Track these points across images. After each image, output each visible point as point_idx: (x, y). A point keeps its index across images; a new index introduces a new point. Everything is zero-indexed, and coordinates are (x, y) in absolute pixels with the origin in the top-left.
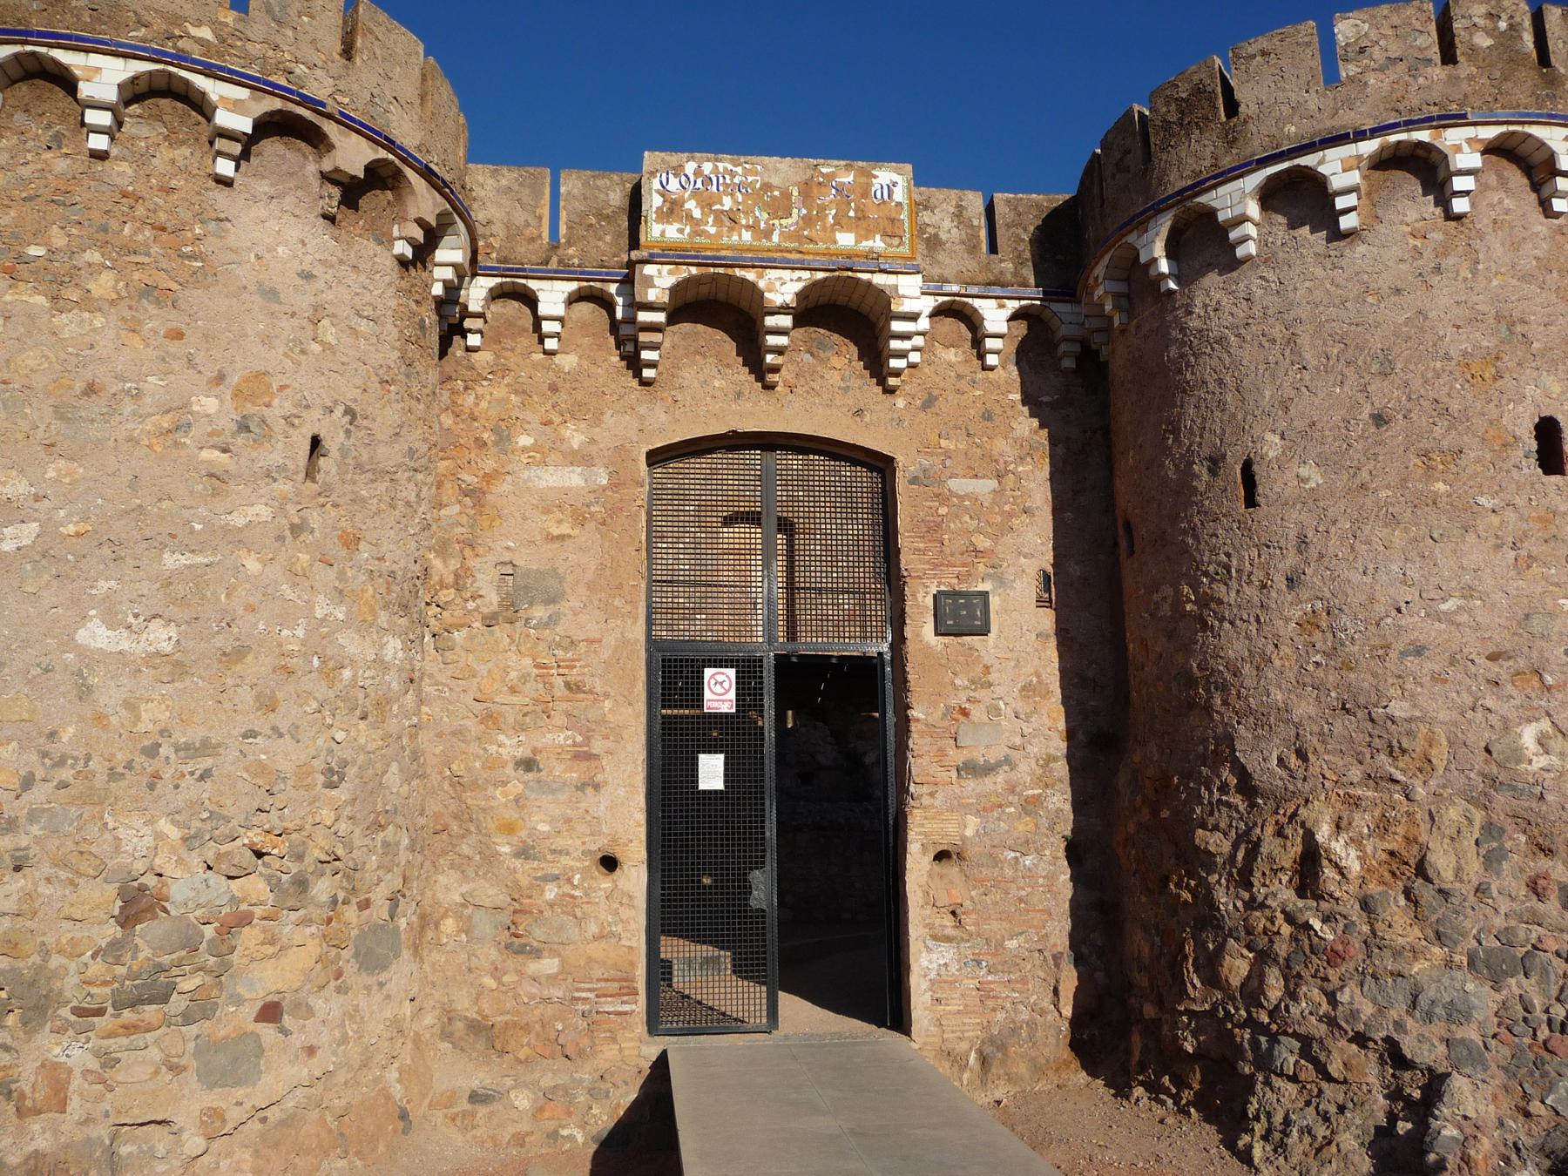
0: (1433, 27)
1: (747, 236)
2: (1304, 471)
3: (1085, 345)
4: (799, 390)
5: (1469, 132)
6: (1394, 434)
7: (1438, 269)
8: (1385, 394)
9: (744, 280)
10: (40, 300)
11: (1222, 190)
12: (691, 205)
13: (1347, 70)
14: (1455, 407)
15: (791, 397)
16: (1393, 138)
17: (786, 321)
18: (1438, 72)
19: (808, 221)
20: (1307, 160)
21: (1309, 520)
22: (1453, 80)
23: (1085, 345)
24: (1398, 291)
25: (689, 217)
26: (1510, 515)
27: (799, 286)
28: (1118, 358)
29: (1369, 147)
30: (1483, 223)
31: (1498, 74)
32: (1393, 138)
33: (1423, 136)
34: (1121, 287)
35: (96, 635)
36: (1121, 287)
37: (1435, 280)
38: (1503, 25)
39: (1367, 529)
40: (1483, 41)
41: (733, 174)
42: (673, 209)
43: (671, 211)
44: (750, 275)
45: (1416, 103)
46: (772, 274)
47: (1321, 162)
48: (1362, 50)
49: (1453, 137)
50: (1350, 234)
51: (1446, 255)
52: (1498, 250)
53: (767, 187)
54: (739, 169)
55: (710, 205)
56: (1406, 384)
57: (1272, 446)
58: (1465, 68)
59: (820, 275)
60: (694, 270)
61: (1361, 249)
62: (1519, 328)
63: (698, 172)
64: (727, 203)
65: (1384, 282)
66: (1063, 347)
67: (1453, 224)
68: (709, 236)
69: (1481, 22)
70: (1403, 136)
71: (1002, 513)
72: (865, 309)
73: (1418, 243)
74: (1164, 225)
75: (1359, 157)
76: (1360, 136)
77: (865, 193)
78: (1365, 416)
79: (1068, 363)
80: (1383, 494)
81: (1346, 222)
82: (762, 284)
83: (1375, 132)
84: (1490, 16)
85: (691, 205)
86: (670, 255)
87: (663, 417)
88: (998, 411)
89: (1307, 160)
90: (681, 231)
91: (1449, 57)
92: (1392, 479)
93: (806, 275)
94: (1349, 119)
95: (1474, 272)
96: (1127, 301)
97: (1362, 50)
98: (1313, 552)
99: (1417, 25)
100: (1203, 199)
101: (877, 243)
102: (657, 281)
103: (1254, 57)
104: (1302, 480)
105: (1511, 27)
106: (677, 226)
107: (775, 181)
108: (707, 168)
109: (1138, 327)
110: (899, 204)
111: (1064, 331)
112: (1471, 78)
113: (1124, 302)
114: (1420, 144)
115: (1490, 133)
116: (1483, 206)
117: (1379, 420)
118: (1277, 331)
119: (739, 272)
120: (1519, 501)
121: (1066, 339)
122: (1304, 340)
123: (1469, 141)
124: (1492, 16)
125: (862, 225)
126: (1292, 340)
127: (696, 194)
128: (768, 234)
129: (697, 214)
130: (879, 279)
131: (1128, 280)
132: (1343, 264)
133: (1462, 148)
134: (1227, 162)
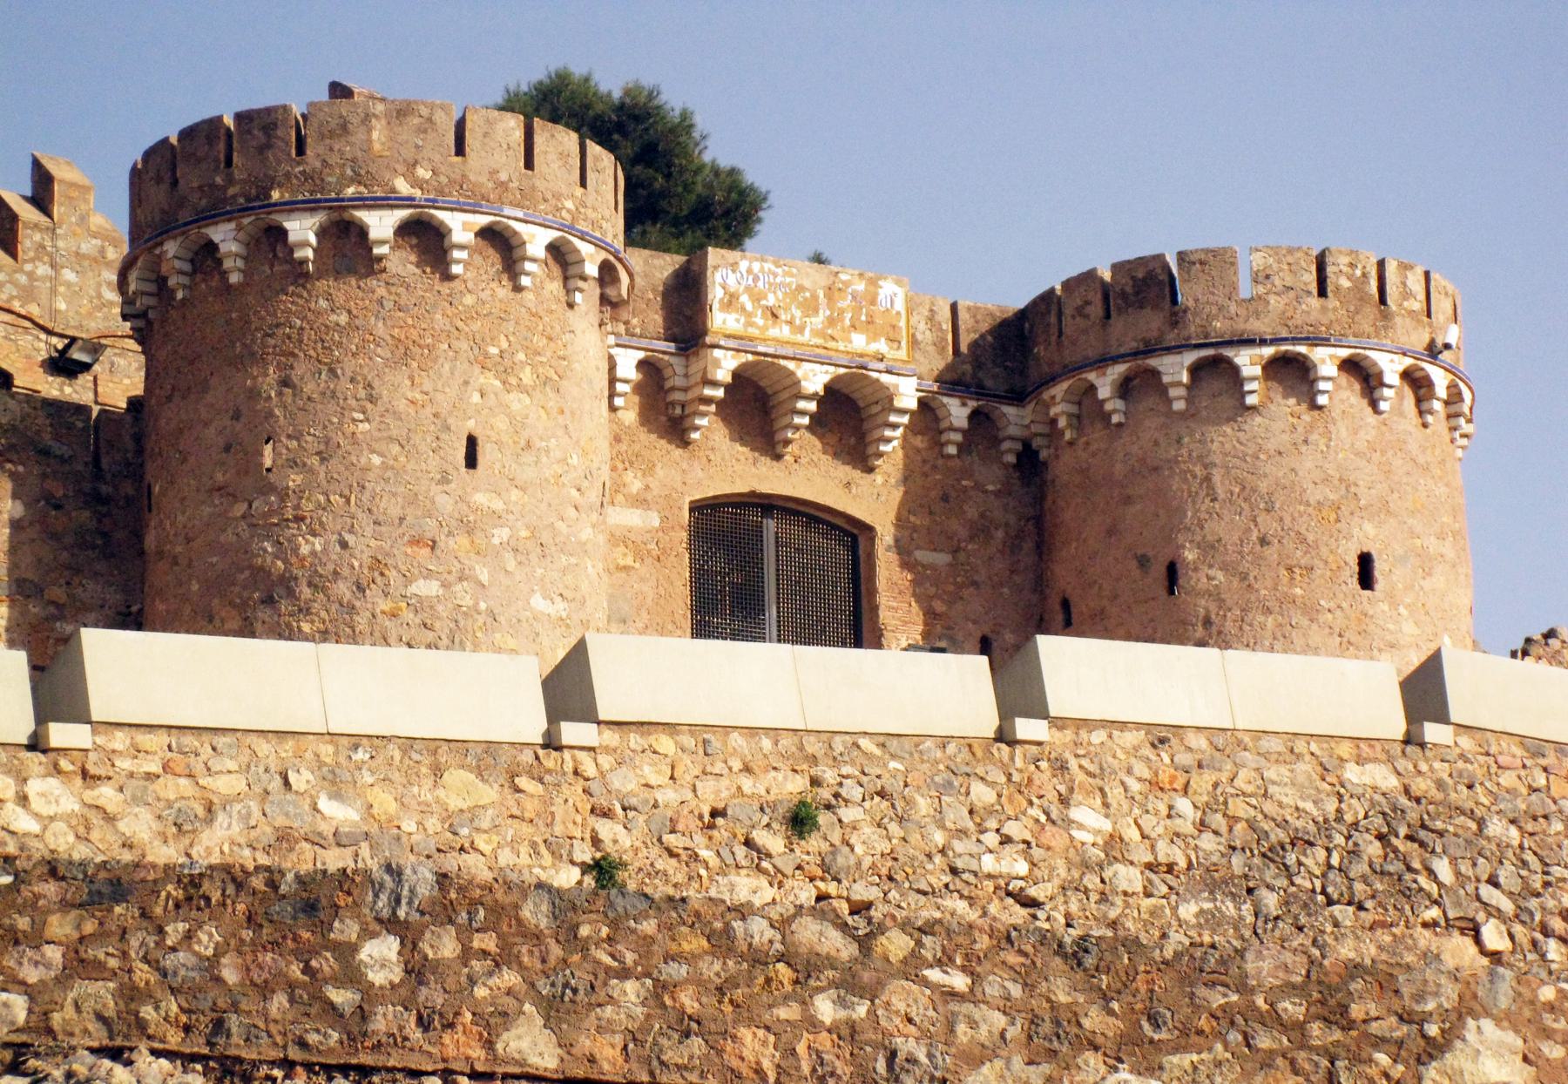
0: (1314, 268)
1: (786, 329)
2: (1212, 572)
3: (1027, 444)
4: (803, 461)
5: (1332, 350)
6: (1271, 553)
7: (1306, 441)
8: (1268, 524)
9: (785, 368)
10: (497, 383)
12: (744, 299)
14: (1311, 538)
15: (796, 466)
16: (1284, 348)
18: (1314, 302)
19: (831, 321)
20: (1228, 352)
21: (1213, 607)
22: (1324, 309)
23: (1027, 444)
25: (743, 309)
26: (1338, 613)
27: (826, 378)
28: (1063, 468)
29: (1268, 351)
30: (1336, 413)
31: (1352, 308)
33: (1302, 349)
34: (1074, 409)
35: (539, 603)
36: (1074, 409)
37: (1304, 448)
38: (1358, 273)
39: (1250, 616)
40: (1345, 283)
41: (776, 275)
42: (731, 302)
43: (730, 302)
44: (791, 365)
45: (1299, 322)
46: (806, 365)
48: (1267, 277)
50: (1253, 408)
52: (1344, 433)
53: (800, 288)
54: (779, 271)
55: (759, 300)
56: (1281, 519)
57: (1190, 555)
58: (1332, 302)
59: (842, 371)
60: (750, 357)
61: (1258, 419)
62: (1353, 489)
63: (749, 271)
64: (771, 300)
65: (1271, 446)
66: (1006, 445)
67: (1316, 413)
68: (758, 327)
69: (1345, 269)
70: (1290, 348)
71: (955, 583)
72: (855, 396)
73: (1295, 421)
75: (1261, 357)
76: (1263, 342)
77: (873, 302)
78: (1254, 538)
79: (1011, 459)
80: (1263, 592)
81: (1251, 400)
82: (799, 374)
83: (1275, 341)
84: (1351, 265)
85: (744, 299)
87: (701, 474)
88: (954, 494)
90: (738, 321)
91: (1322, 293)
92: (1269, 583)
93: (832, 369)
94: (1258, 326)
95: (1328, 447)
96: (1077, 420)
97: (1267, 277)
98: (1214, 629)
99: (1304, 264)
100: (1153, 362)
101: (882, 346)
102: (724, 363)
104: (1209, 578)
105: (1364, 275)
106: (734, 316)
107: (807, 283)
108: (756, 266)
109: (1087, 443)
110: (898, 313)
111: (1012, 430)
112: (1335, 309)
113: (1075, 421)
114: (1299, 354)
115: (1344, 353)
116: (1336, 401)
117: (1263, 541)
118: (1198, 470)
119: (782, 362)
120: (1344, 605)
121: (1012, 438)
122: (1217, 478)
123: (1332, 357)
124: (1351, 265)
125: (871, 327)
126: (1208, 478)
127: (748, 289)
128: (801, 330)
129: (749, 307)
130: (886, 379)
131: (1079, 403)
132: (1246, 427)
133: (1326, 361)
134: (1171, 338)
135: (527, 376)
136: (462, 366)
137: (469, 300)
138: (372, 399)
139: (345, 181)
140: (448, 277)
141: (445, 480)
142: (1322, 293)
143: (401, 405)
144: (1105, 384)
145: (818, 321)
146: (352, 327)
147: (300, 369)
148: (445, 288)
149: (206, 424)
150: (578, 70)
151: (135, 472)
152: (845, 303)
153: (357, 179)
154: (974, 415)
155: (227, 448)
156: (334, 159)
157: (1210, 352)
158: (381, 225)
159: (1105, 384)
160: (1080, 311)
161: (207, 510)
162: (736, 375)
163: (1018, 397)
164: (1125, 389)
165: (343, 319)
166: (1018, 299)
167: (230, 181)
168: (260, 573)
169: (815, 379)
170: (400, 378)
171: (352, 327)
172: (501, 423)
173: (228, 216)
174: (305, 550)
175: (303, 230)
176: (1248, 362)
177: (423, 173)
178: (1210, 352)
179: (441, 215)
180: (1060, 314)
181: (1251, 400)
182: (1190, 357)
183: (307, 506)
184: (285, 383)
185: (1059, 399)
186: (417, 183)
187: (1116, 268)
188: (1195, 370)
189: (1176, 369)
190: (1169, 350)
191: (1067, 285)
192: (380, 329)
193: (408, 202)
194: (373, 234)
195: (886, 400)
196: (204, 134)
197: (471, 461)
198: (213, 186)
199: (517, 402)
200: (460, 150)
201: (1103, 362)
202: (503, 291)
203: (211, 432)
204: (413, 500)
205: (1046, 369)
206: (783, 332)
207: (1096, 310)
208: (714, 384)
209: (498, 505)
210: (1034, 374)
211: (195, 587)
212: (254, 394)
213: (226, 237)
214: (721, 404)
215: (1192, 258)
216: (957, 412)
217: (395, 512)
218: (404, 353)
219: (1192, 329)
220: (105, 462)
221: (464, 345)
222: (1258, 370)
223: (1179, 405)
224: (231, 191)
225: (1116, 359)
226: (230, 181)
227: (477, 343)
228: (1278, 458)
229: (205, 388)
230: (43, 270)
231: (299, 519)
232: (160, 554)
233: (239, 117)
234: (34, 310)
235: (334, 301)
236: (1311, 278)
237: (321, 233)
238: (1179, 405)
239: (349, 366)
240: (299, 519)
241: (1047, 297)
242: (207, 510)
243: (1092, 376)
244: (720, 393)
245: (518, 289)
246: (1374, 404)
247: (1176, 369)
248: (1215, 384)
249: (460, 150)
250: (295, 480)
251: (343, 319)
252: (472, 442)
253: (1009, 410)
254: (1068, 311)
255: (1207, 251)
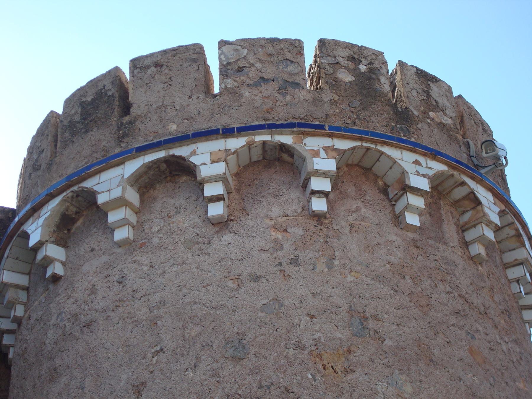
5: (327, 142)
7: (295, 261)
11: (105, 176)
20: (182, 151)
24: (256, 279)
32: (259, 138)
33: (287, 139)
37: (292, 270)
38: (363, 68)
47: (194, 153)
49: (313, 143)
51: (304, 249)
61: (227, 237)
62: (371, 324)
70: (267, 138)
73: (280, 236)
75: (227, 152)
76: (228, 132)
83: (242, 130)
89: (182, 151)
95: (330, 266)
97: (240, 70)
103: (148, 67)
112: (332, 102)
114: (283, 147)
116: (341, 211)
123: (326, 149)
157: (161, 154)
178: (161, 154)
215: (147, 62)
228: (253, 285)
255: (164, 52)
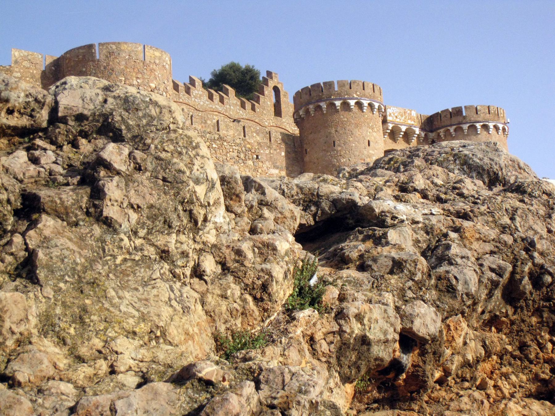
13: (479, 113)
17: (403, 133)
18: (488, 115)
19: (405, 118)
29: (482, 124)
50: (479, 134)
58: (491, 115)
64: (396, 115)
66: (430, 140)
74: (454, 127)
86: (392, 122)
96: (445, 136)
100: (461, 126)
101: (413, 123)
111: (431, 137)
130: (414, 128)
134: (464, 121)
135: (375, 130)
136: (366, 128)
137: (366, 116)
138: (352, 134)
139: (345, 95)
140: (363, 112)
141: (365, 148)
142: (489, 113)
143: (357, 135)
144: (452, 129)
145: (403, 118)
146: (348, 121)
147: (339, 129)
148: (363, 114)
149: (320, 138)
150: (236, 62)
151: (301, 146)
152: (407, 115)
153: (347, 94)
154: (425, 135)
155: (325, 143)
156: (343, 91)
158: (352, 103)
159: (452, 129)
160: (445, 116)
161: (321, 154)
162: (392, 128)
163: (432, 131)
164: (455, 130)
165: (346, 119)
166: (430, 113)
167: (323, 95)
168: (334, 165)
169: (404, 128)
170: (356, 130)
171: (348, 121)
172: (373, 138)
173: (324, 101)
174: (342, 161)
175: (338, 103)
176: (478, 125)
177: (358, 93)
179: (362, 101)
180: (441, 117)
181: (479, 132)
182: (468, 125)
183: (342, 153)
184: (336, 131)
185: (442, 132)
186: (357, 95)
187: (452, 109)
188: (469, 127)
189: (465, 127)
190: (464, 123)
191: (442, 111)
192: (353, 121)
193: (356, 99)
194: (351, 104)
195: (414, 132)
196: (317, 86)
197: (369, 145)
198: (319, 95)
199: (375, 134)
200: (364, 89)
201: (451, 125)
202: (371, 115)
203: (322, 139)
204: (360, 152)
205: (437, 127)
206: (398, 120)
207: (449, 116)
208: (388, 130)
209: (373, 153)
210: (434, 127)
211: (320, 168)
212: (330, 133)
213: (324, 105)
214: (389, 133)
216: (423, 134)
217: (358, 154)
218: (357, 126)
219: (468, 120)
220: (296, 145)
221: (366, 124)
222: (480, 127)
223: (466, 133)
224: (323, 96)
225: (454, 125)
226: (323, 95)
227: (368, 124)
229: (319, 132)
230: (228, 106)
231: (341, 155)
232: (310, 162)
233: (324, 83)
234: (227, 114)
235: (344, 116)
236: (487, 111)
237: (341, 104)
238: (466, 133)
239: (348, 128)
240: (341, 155)
241: (438, 113)
242: (321, 154)
243: (449, 128)
244: (389, 131)
245: (373, 114)
246: (498, 133)
247: (465, 127)
248: (471, 129)
249: (364, 89)
250: (339, 148)
251: (346, 119)
252: (369, 141)
253: (430, 134)
254: (442, 116)
